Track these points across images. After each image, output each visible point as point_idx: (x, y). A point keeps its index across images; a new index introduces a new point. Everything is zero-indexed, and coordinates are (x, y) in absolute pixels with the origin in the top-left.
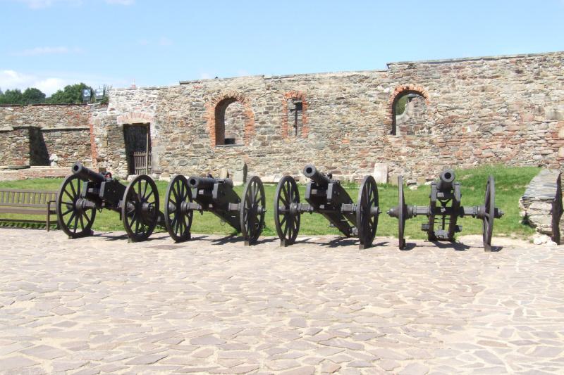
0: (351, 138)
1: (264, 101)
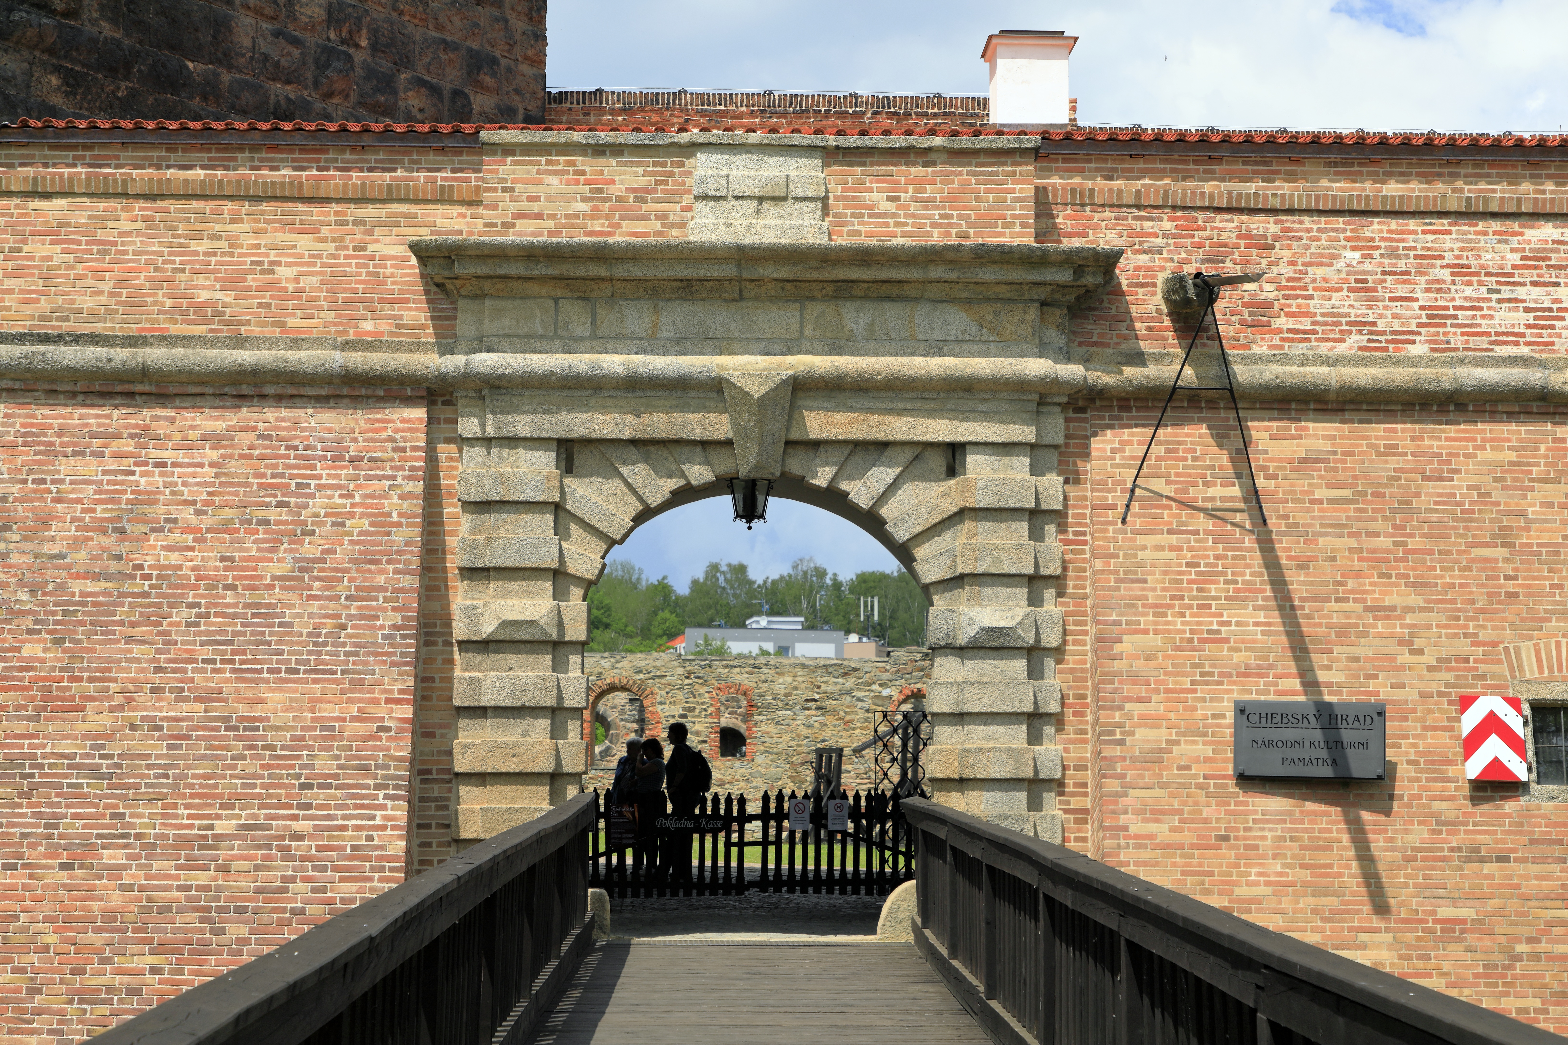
1: (680, 695)
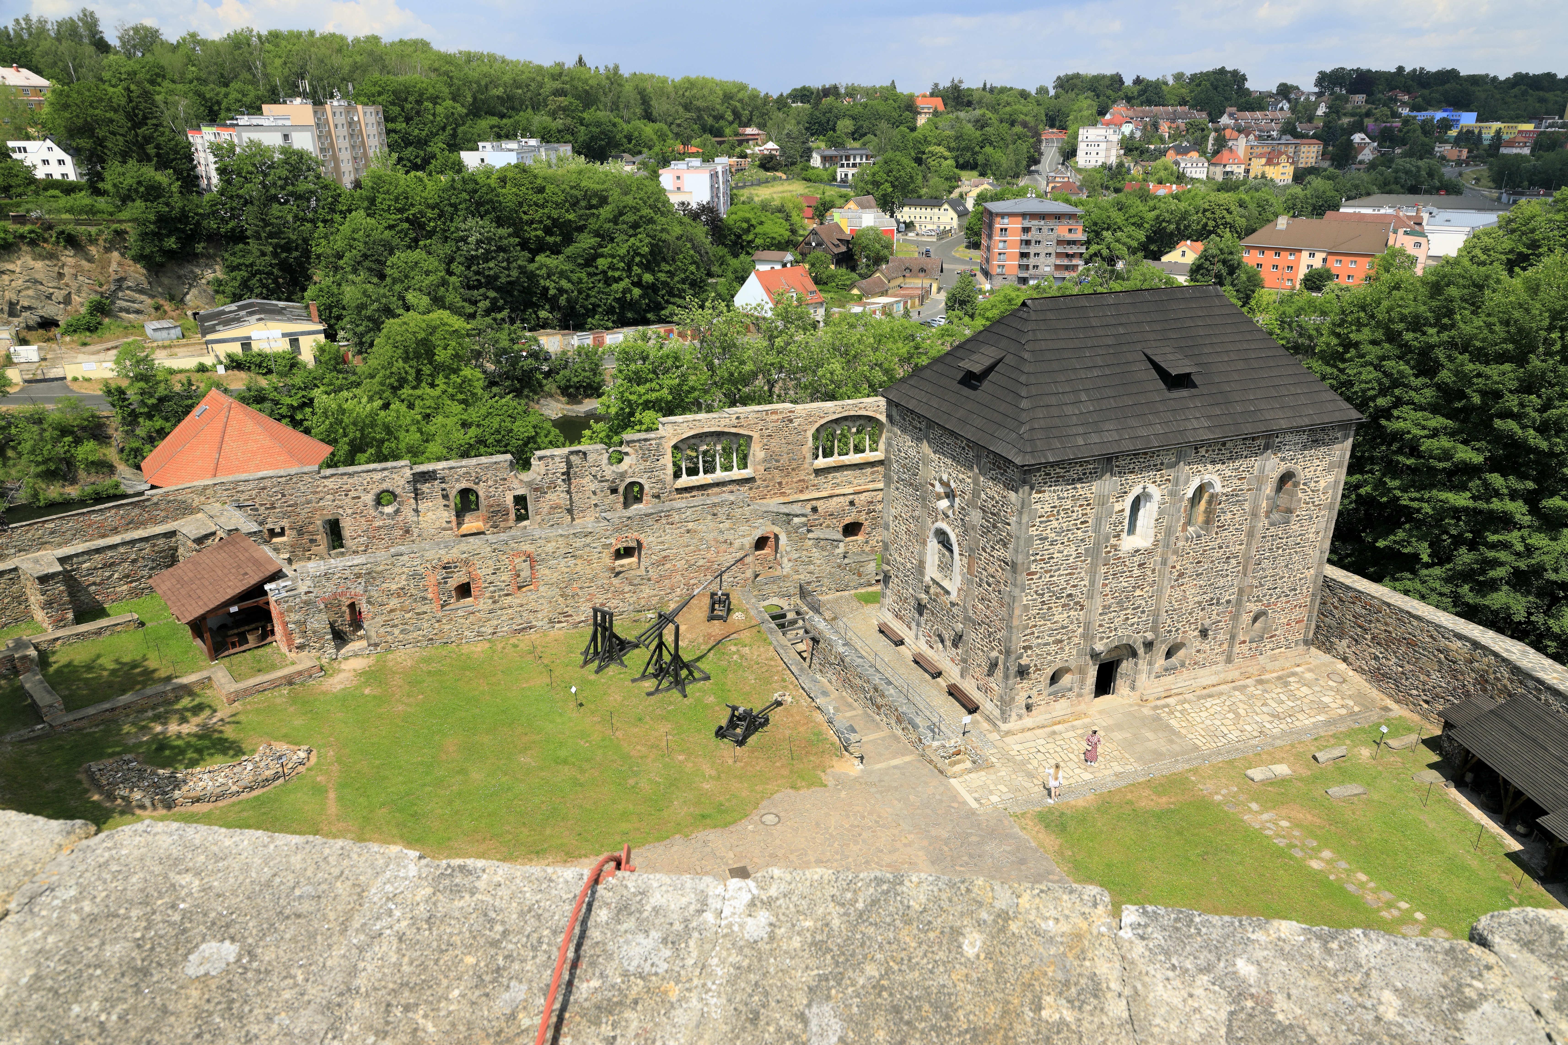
1: (490, 562)
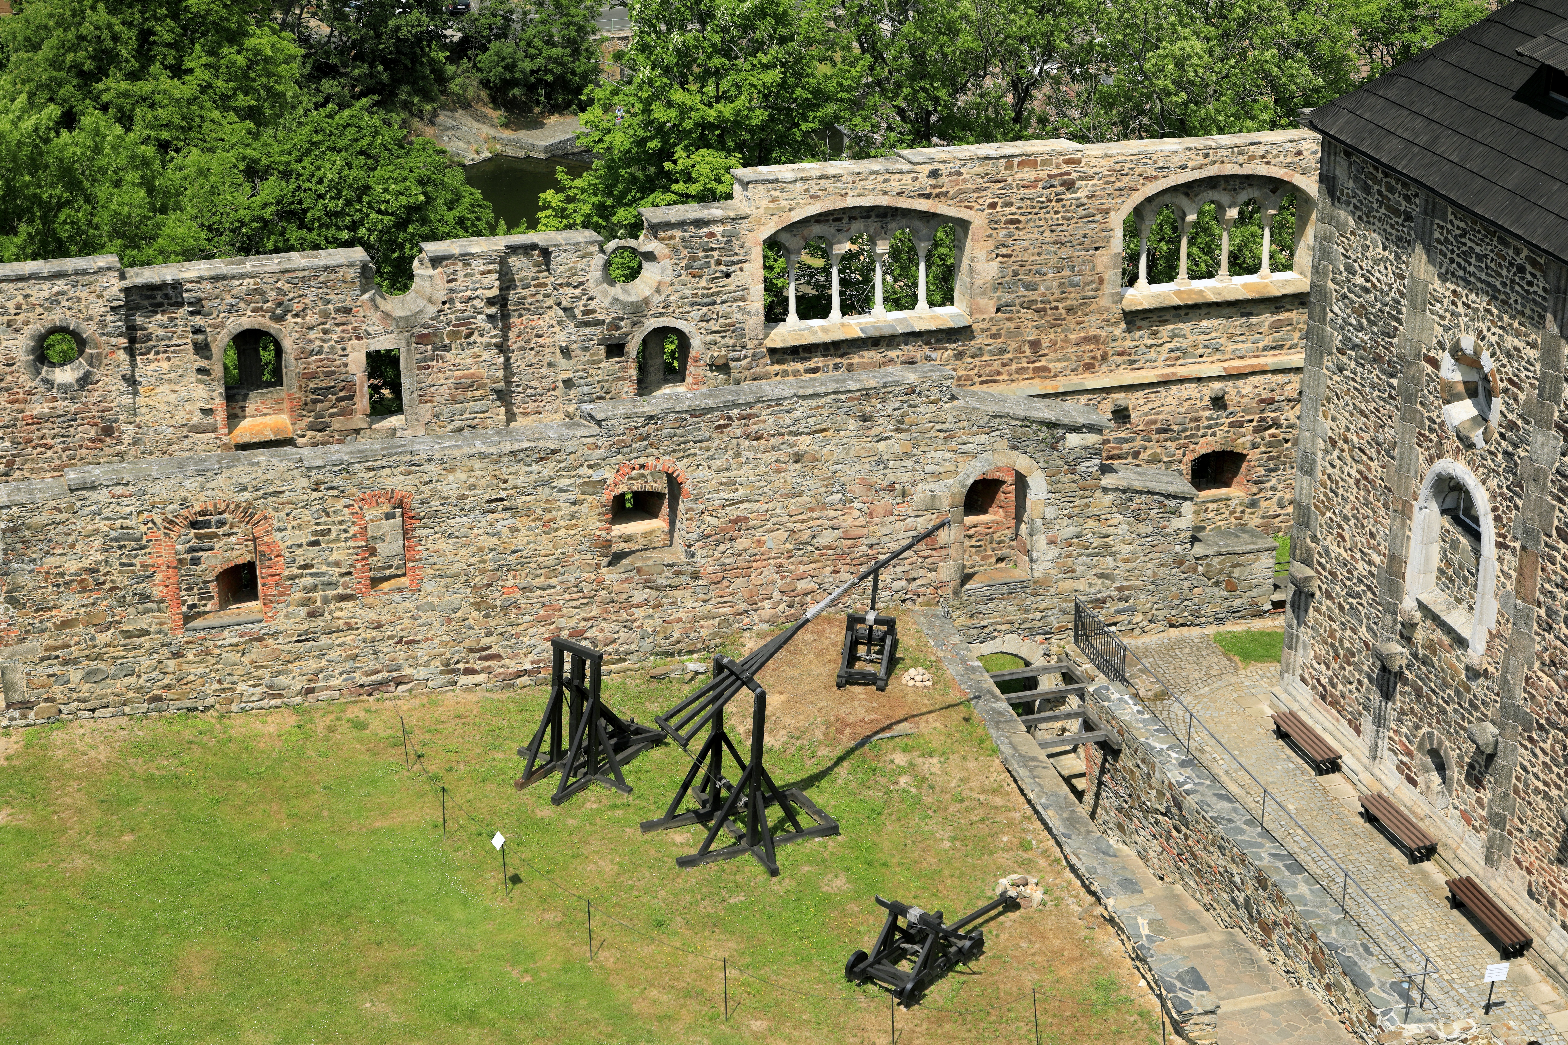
0: (523, 584)
1: (306, 516)
